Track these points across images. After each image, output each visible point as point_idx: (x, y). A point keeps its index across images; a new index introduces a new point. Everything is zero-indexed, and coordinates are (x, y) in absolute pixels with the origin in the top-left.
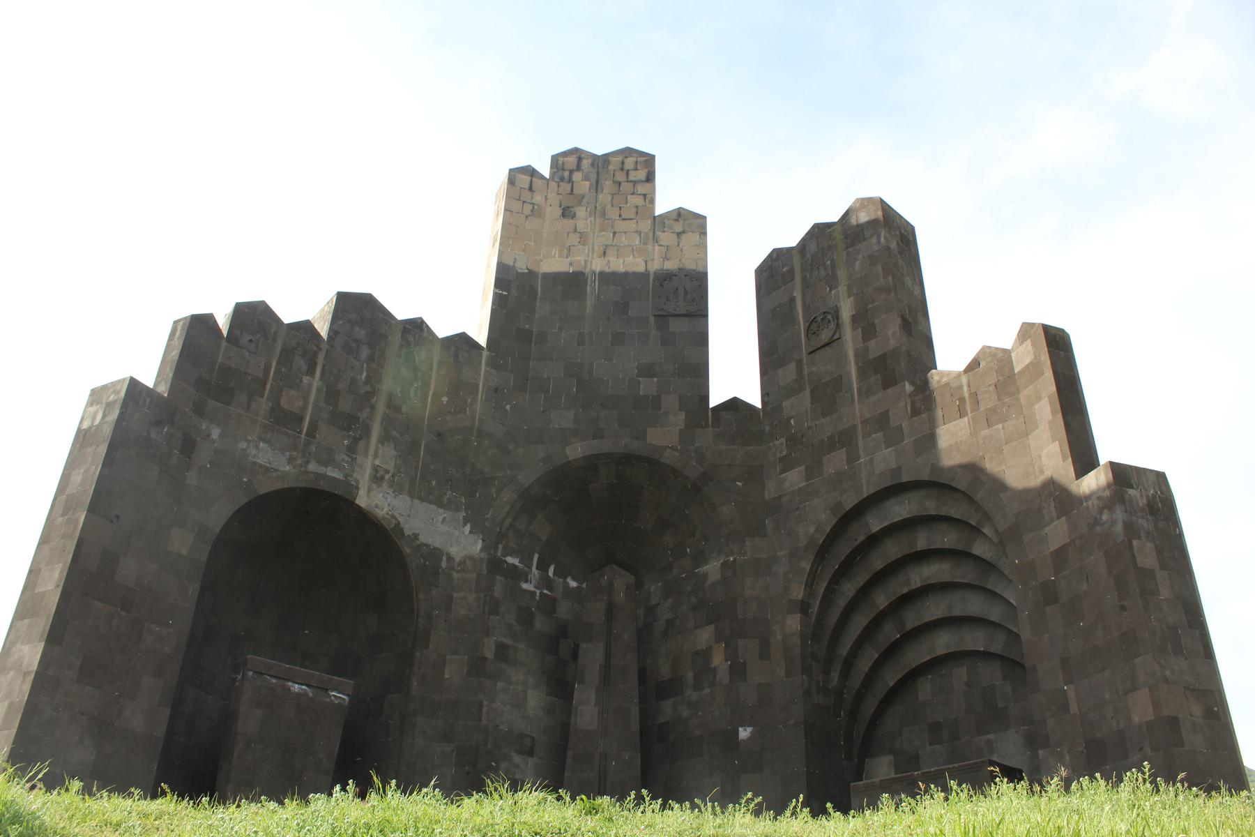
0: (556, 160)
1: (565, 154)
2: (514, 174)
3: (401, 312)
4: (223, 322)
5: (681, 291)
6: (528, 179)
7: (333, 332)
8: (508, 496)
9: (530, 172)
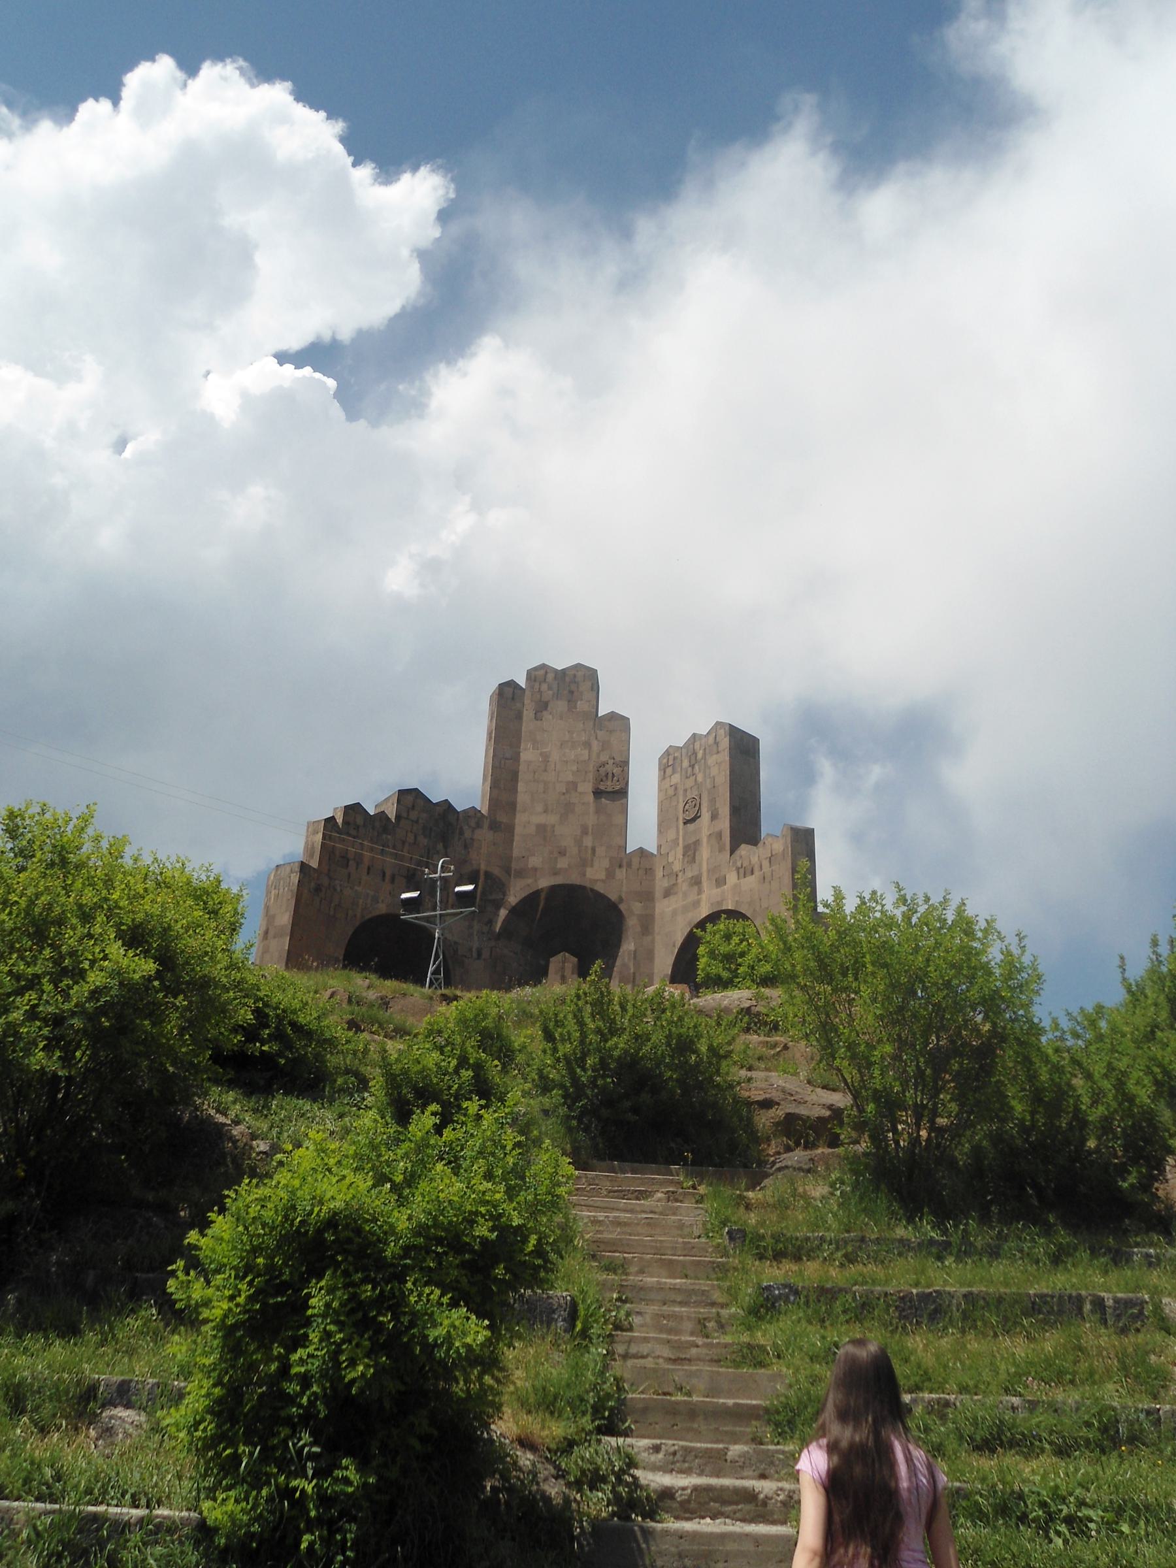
0: (529, 672)
1: (535, 669)
2: (502, 687)
3: (435, 798)
4: (340, 821)
5: (610, 775)
6: (511, 690)
7: (398, 817)
8: (503, 913)
9: (511, 684)
